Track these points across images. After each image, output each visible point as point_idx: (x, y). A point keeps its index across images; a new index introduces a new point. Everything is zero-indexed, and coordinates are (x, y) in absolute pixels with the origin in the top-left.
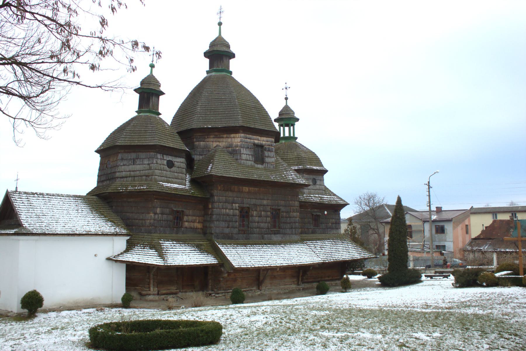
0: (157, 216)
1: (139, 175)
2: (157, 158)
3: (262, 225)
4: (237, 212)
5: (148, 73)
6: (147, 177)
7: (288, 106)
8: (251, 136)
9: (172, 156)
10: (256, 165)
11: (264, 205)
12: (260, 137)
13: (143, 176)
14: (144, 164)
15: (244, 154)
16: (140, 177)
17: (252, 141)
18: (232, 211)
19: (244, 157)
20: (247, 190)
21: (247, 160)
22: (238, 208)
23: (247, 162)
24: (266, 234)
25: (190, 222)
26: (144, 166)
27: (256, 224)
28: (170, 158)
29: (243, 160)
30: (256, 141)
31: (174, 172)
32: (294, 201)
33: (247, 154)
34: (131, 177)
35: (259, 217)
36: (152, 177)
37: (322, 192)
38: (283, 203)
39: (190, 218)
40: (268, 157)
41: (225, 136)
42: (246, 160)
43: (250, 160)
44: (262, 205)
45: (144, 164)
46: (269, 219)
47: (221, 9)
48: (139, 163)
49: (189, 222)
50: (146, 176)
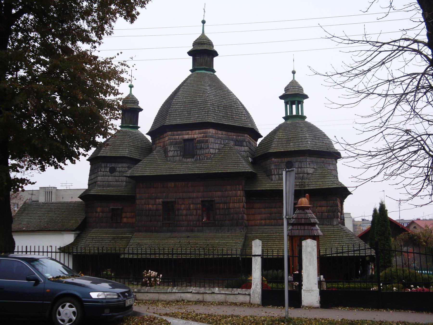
0: (97, 215)
2: (101, 167)
3: (191, 218)
4: (160, 207)
5: (129, 93)
7: (295, 80)
8: (179, 132)
9: (115, 163)
10: (185, 160)
11: (193, 198)
12: (191, 131)
15: (172, 151)
17: (180, 137)
18: (155, 206)
19: (170, 154)
20: (173, 186)
21: (175, 156)
22: (161, 203)
23: (175, 158)
24: (195, 227)
25: (129, 218)
27: (184, 217)
28: (113, 165)
29: (170, 157)
30: (186, 137)
31: (115, 176)
32: (235, 191)
33: (174, 151)
35: (187, 210)
37: (303, 176)
38: (219, 193)
39: (128, 215)
40: (201, 148)
42: (173, 156)
43: (177, 156)
44: (190, 198)
46: (199, 212)
49: (127, 218)
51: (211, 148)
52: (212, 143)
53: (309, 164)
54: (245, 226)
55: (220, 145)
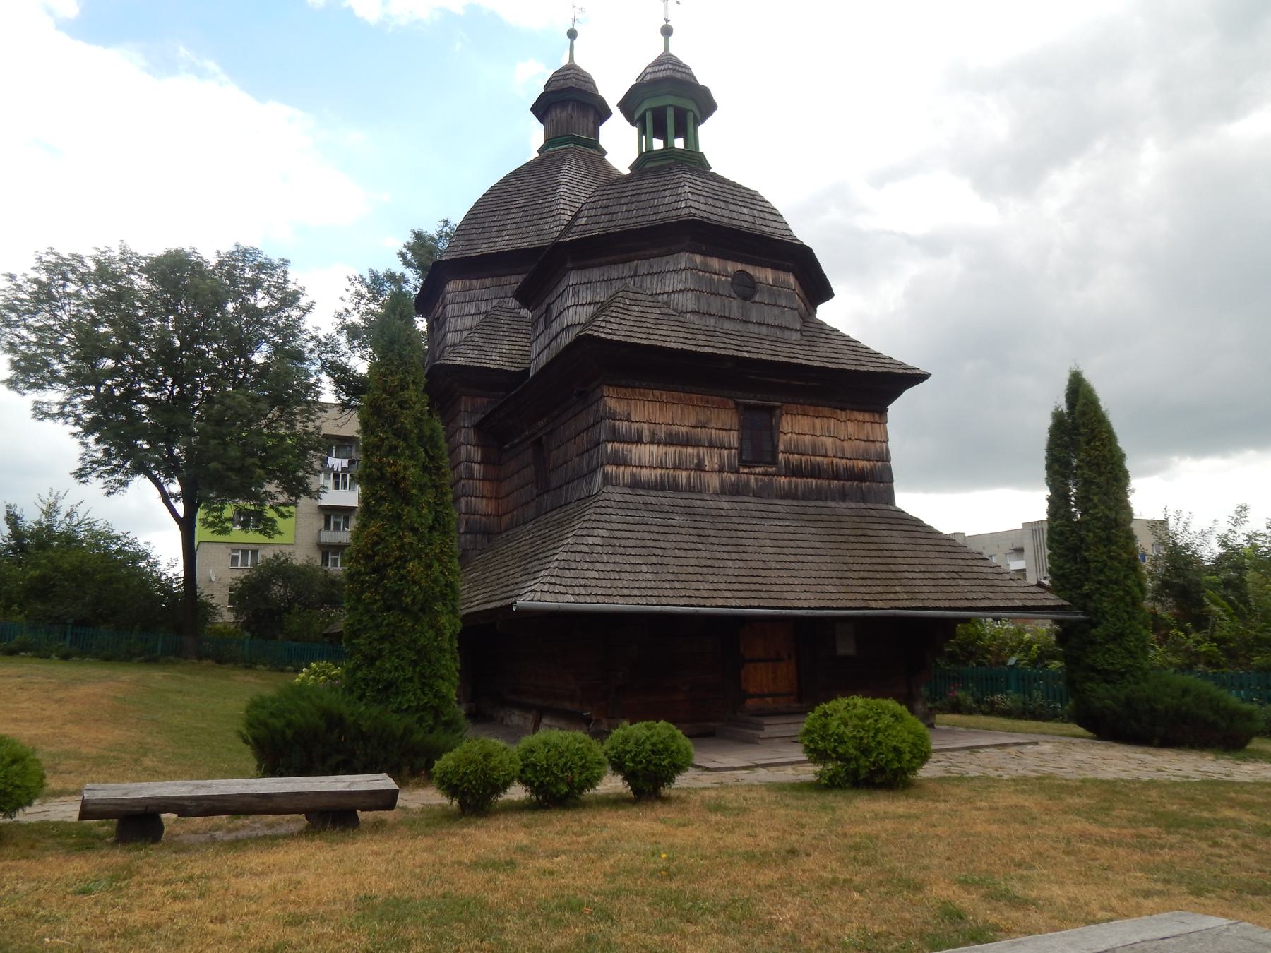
51: (449, 332)
52: (453, 317)
53: (576, 294)
54: (465, 533)
55: (475, 317)
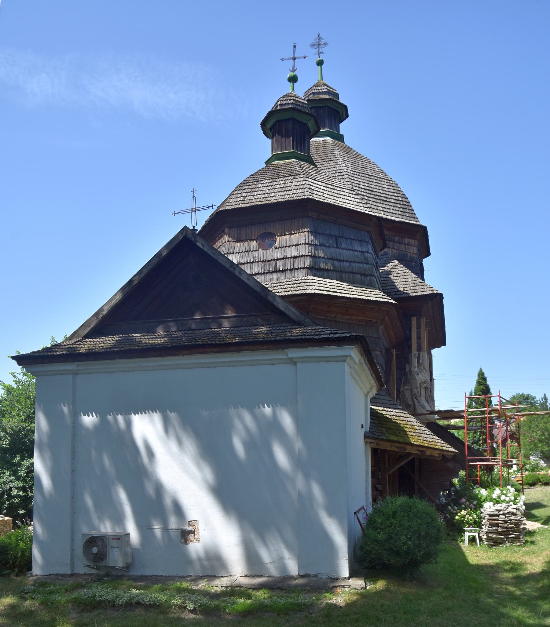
1: (349, 269)
6: (363, 277)
13: (356, 273)
14: (355, 251)
16: (351, 275)
26: (356, 253)
34: (336, 271)
36: (371, 278)
41: (397, 239)
45: (355, 251)
47: (319, 40)
48: (347, 247)
50: (362, 274)
